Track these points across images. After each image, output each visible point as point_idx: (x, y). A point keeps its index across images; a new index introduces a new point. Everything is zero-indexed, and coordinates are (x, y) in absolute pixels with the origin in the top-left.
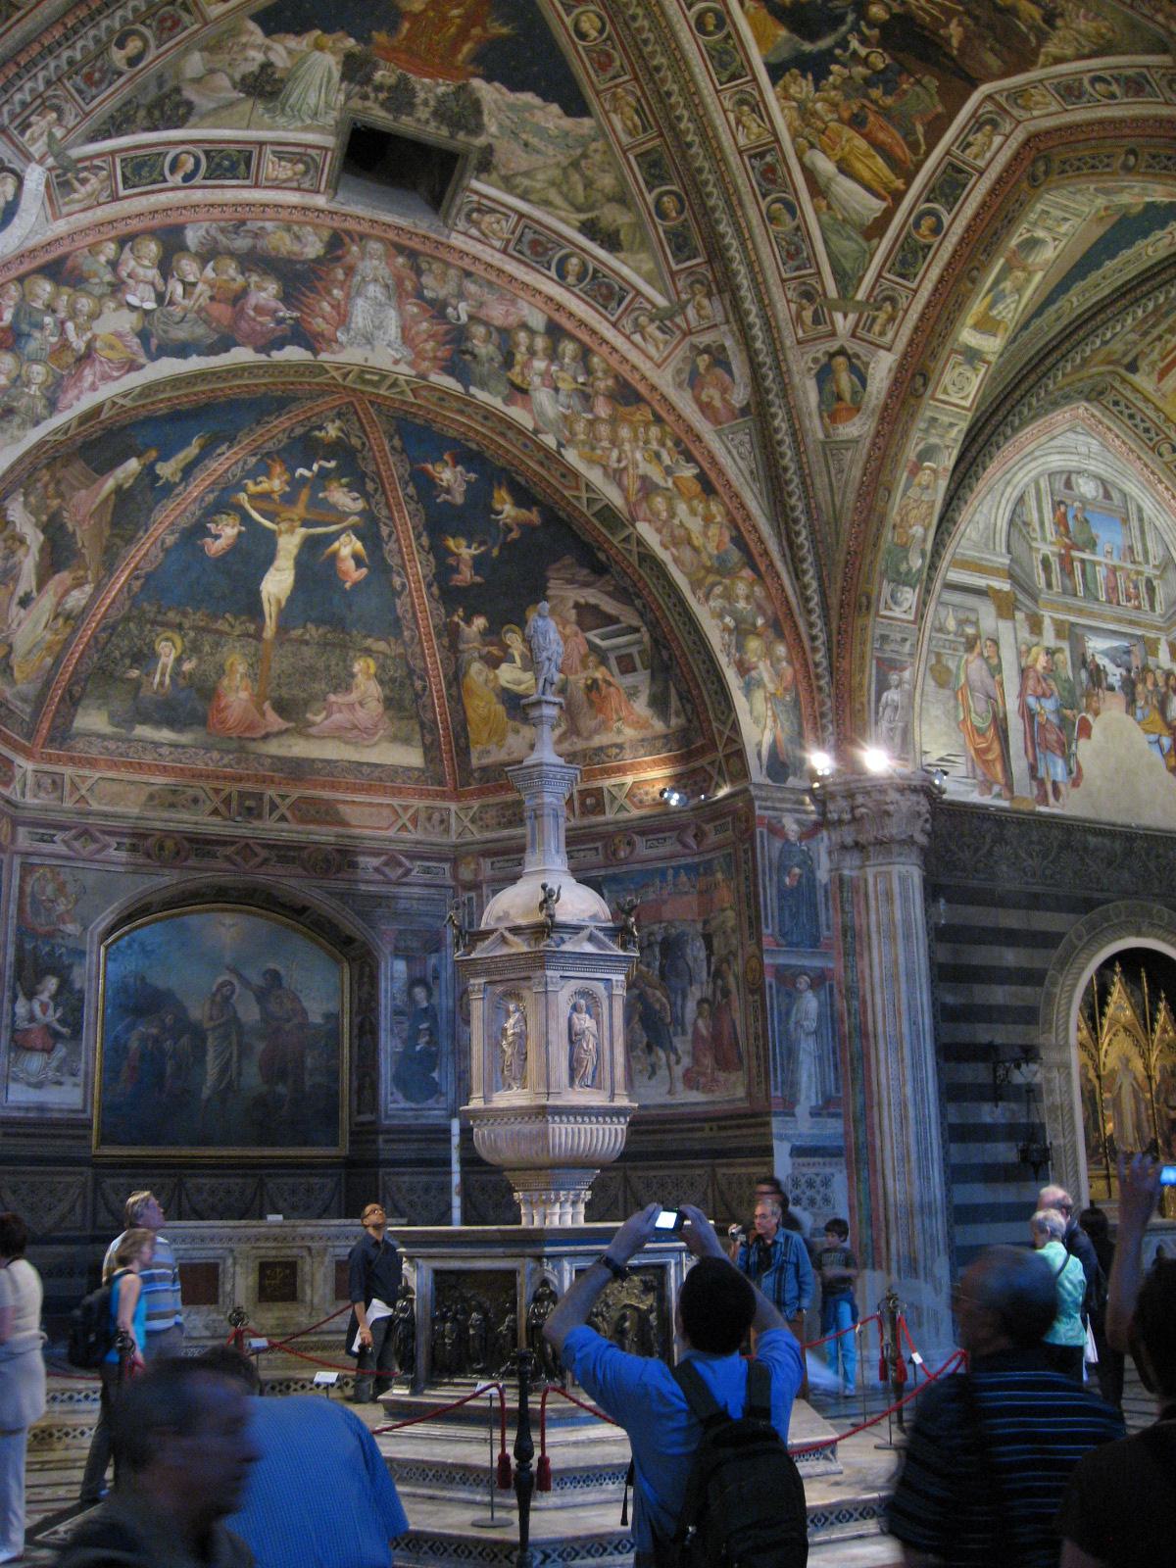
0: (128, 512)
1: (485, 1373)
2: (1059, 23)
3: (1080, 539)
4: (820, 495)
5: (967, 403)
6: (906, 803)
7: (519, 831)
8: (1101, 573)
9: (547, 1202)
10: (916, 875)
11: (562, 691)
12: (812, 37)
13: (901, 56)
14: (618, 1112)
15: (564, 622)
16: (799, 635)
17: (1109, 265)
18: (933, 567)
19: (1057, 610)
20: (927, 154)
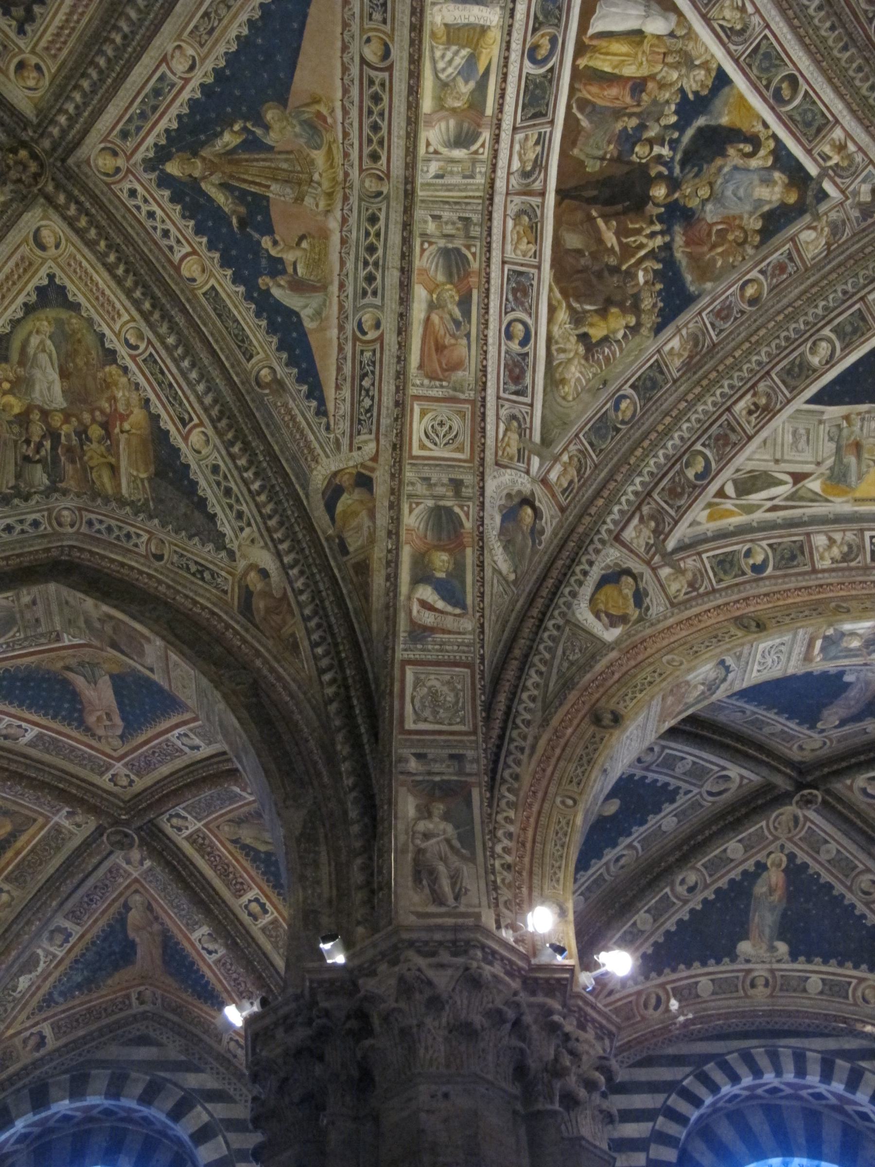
2: (581, 349)
12: (700, 130)
13: (626, 169)
20: (569, 107)
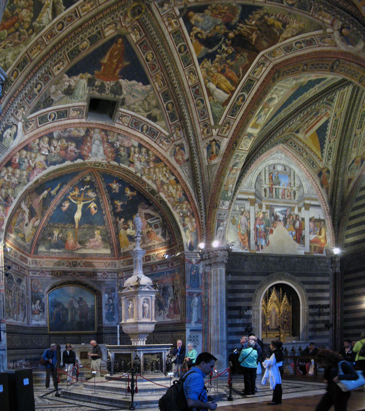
0: (46, 202)
1: (125, 372)
3: (276, 182)
4: (206, 180)
5: (247, 149)
6: (222, 253)
7: (131, 266)
8: (281, 191)
9: (137, 341)
10: (224, 269)
11: (141, 234)
14: (153, 323)
15: (142, 218)
16: (198, 216)
17: (294, 102)
18: (234, 195)
19: (266, 202)
